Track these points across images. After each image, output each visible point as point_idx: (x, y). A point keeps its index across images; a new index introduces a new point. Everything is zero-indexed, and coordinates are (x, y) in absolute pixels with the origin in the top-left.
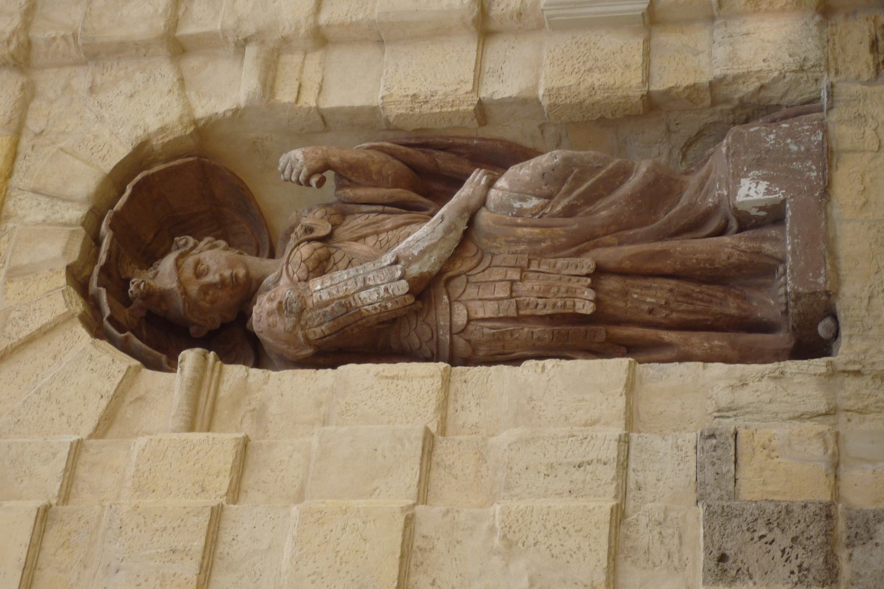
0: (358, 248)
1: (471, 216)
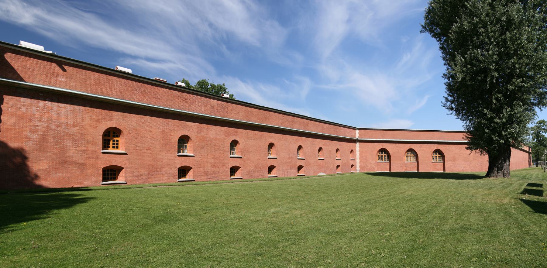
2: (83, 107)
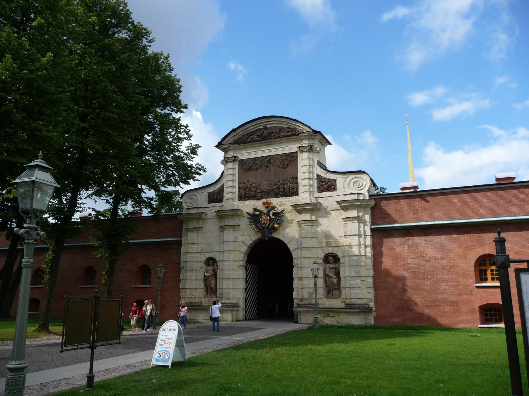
2: (294, 269)
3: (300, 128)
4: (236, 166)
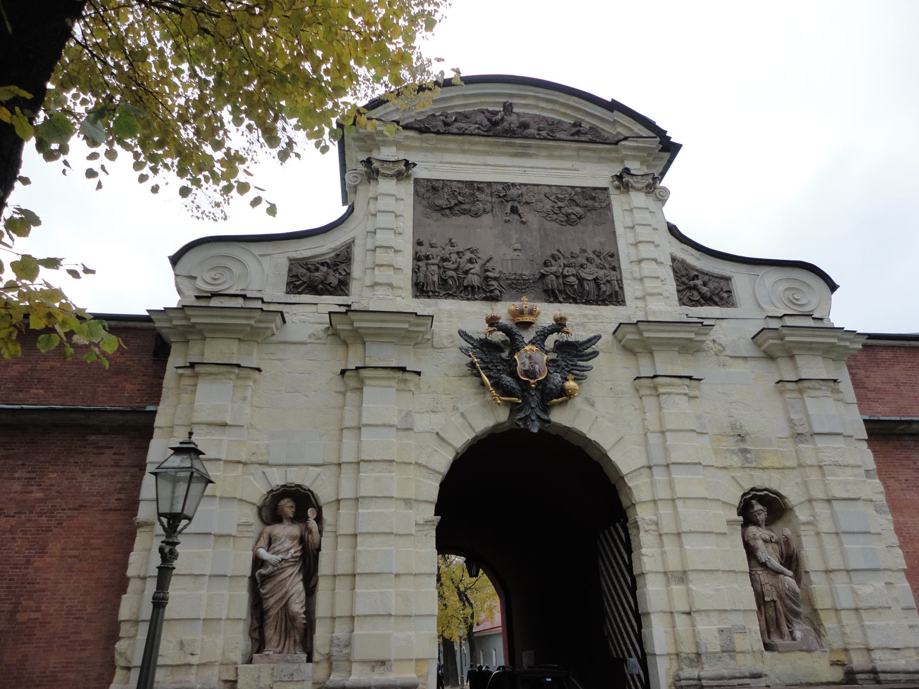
0: (770, 548)
1: (782, 573)
3: (620, 129)
4: (406, 190)
